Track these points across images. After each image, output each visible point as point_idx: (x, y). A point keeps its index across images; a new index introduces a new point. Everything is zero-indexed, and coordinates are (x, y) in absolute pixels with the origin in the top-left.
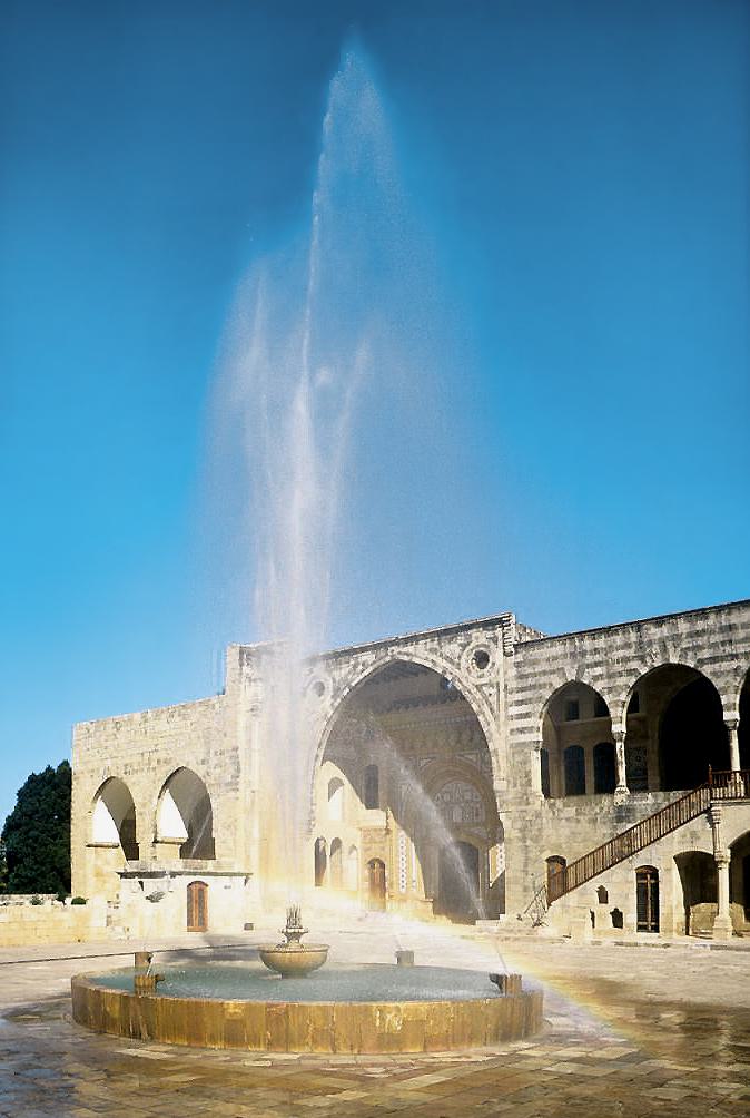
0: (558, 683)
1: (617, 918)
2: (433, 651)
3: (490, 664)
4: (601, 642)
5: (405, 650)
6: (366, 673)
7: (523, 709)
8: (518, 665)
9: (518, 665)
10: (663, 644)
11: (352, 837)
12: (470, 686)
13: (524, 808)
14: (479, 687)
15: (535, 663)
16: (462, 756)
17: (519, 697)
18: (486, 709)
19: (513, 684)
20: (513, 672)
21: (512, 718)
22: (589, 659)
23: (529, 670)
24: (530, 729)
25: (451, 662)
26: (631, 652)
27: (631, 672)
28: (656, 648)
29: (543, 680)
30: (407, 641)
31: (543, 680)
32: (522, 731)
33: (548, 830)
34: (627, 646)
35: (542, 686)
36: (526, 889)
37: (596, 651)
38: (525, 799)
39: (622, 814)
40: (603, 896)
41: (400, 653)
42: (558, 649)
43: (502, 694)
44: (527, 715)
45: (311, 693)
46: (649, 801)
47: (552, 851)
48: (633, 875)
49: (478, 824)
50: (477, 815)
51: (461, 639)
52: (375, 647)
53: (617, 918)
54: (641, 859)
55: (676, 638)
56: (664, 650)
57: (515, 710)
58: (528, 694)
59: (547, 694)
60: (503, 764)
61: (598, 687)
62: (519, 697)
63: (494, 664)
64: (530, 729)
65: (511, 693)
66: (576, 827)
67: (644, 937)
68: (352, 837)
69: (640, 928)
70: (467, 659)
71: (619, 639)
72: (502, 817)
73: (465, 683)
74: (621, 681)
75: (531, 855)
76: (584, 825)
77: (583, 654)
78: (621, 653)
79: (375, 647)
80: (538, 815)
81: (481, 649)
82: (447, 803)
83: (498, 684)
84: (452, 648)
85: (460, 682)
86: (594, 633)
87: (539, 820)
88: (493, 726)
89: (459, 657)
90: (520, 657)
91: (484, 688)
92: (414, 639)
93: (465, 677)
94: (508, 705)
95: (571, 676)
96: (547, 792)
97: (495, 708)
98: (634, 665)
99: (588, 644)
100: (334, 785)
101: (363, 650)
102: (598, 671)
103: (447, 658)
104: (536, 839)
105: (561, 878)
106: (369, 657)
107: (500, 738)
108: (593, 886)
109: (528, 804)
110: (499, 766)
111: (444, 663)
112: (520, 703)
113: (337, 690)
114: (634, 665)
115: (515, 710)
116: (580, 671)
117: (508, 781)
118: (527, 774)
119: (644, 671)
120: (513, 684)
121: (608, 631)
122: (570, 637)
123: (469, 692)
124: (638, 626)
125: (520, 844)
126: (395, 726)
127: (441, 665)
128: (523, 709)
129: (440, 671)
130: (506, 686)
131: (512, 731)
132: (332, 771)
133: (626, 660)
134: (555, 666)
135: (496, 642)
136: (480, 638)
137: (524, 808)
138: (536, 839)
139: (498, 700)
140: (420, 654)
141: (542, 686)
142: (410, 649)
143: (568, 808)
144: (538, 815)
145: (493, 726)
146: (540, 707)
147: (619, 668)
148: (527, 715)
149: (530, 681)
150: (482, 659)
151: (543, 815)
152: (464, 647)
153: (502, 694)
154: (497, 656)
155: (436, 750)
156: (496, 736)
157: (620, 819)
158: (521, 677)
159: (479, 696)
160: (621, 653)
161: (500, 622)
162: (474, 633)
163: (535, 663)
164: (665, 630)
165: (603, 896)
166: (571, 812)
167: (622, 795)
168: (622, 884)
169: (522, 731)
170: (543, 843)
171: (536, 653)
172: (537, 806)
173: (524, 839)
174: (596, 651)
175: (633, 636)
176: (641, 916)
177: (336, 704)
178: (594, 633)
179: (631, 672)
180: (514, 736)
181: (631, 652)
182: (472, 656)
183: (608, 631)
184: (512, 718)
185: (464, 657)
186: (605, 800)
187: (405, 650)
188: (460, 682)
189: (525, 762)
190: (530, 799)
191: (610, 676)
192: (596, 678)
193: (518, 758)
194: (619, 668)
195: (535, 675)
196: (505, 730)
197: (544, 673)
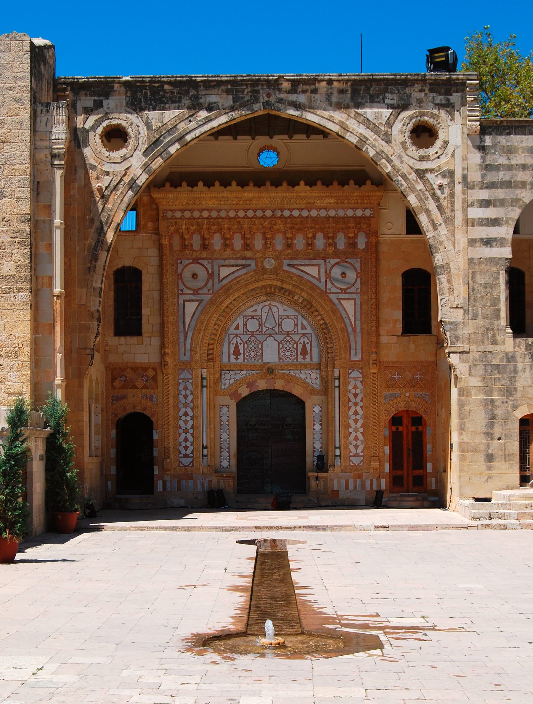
3: (439, 143)
5: (293, 97)
6: (215, 124)
7: (490, 213)
12: (405, 169)
13: (491, 348)
14: (421, 174)
16: (293, 266)
17: (484, 194)
18: (432, 205)
21: (469, 223)
23: (502, 160)
24: (501, 242)
25: (375, 129)
32: (488, 242)
33: (524, 380)
41: (280, 101)
43: (458, 188)
44: (495, 222)
47: (529, 406)
49: (305, 366)
50: (304, 352)
57: (476, 213)
58: (500, 193)
62: (484, 194)
63: (446, 143)
64: (501, 242)
65: (473, 188)
72: (454, 359)
73: (396, 162)
75: (500, 412)
81: (426, 118)
82: (253, 334)
83: (450, 174)
85: (390, 161)
87: (511, 366)
88: (443, 230)
89: (389, 124)
91: (429, 176)
94: (467, 205)
97: (445, 203)
103: (367, 123)
104: (509, 391)
109: (494, 343)
110: (450, 288)
111: (362, 130)
112: (486, 203)
115: (476, 213)
117: (466, 311)
118: (495, 301)
120: (475, 176)
123: (404, 177)
125: (482, 396)
126: (183, 211)
128: (490, 213)
129: (354, 140)
130: (465, 177)
131: (472, 242)
137: (491, 348)
139: (452, 195)
142: (302, 98)
144: (511, 358)
145: (443, 230)
148: (495, 222)
149: (502, 176)
150: (423, 134)
151: (519, 360)
153: (458, 188)
155: (249, 254)
156: (447, 243)
158: (487, 167)
159: (420, 186)
163: (510, 151)
169: (488, 242)
170: (518, 395)
173: (488, 391)
177: (155, 166)
182: (410, 126)
184: (469, 223)
185: (398, 126)
187: (293, 97)
188: (390, 161)
190: (499, 338)
193: (481, 279)
195: (510, 168)
196: (462, 240)
197: (524, 167)
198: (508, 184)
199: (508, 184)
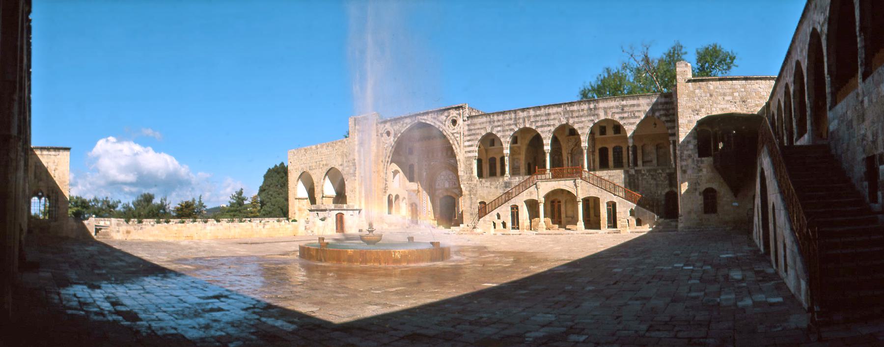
0: (484, 133)
1: (504, 224)
2: (435, 118)
4: (501, 117)
7: (470, 143)
8: (468, 125)
9: (468, 125)
10: (524, 119)
11: (403, 194)
15: (474, 124)
17: (468, 138)
19: (466, 133)
20: (466, 128)
22: (496, 124)
23: (472, 127)
24: (473, 151)
26: (512, 122)
27: (511, 130)
28: (521, 121)
29: (478, 131)
30: (424, 114)
31: (478, 131)
32: (469, 152)
34: (510, 119)
35: (478, 134)
36: (472, 214)
37: (499, 121)
38: (470, 179)
39: (507, 185)
40: (499, 216)
42: (484, 119)
44: (471, 146)
45: (385, 135)
46: (517, 180)
48: (510, 209)
51: (446, 114)
52: (410, 117)
53: (504, 224)
54: (512, 202)
55: (529, 117)
56: (524, 121)
57: (467, 144)
58: (472, 137)
59: (479, 137)
60: (462, 165)
61: (499, 135)
62: (468, 138)
64: (473, 151)
66: (489, 190)
67: (516, 232)
68: (403, 194)
69: (513, 228)
70: (449, 123)
71: (507, 116)
72: (462, 186)
74: (507, 133)
76: (493, 190)
77: (494, 122)
78: (508, 122)
79: (410, 117)
80: (476, 185)
84: (443, 117)
86: (498, 113)
90: (469, 122)
92: (427, 113)
93: (448, 130)
95: (489, 131)
96: (480, 175)
98: (513, 127)
99: (496, 118)
100: (395, 173)
101: (406, 117)
102: (499, 128)
104: (475, 195)
105: (483, 210)
106: (408, 120)
107: (461, 156)
108: (495, 212)
111: (438, 123)
112: (469, 141)
113: (395, 134)
114: (513, 127)
115: (467, 144)
116: (492, 128)
118: (472, 169)
119: (516, 129)
121: (504, 113)
122: (489, 115)
124: (515, 111)
127: (438, 124)
128: (470, 143)
132: (394, 167)
133: (510, 125)
134: (483, 126)
135: (459, 114)
136: (454, 113)
138: (475, 195)
140: (429, 120)
141: (478, 134)
142: (425, 117)
143: (486, 183)
144: (476, 185)
146: (476, 142)
147: (507, 128)
148: (471, 146)
149: (473, 132)
150: (454, 122)
152: (447, 117)
154: (460, 121)
157: (506, 187)
158: (469, 130)
160: (508, 122)
161: (461, 107)
162: (451, 111)
163: (474, 124)
164: (525, 114)
165: (499, 216)
166: (488, 184)
167: (507, 176)
168: (505, 211)
169: (469, 152)
171: (476, 120)
172: (475, 182)
174: (499, 121)
175: (513, 115)
176: (513, 223)
178: (498, 113)
179: (511, 130)
180: (466, 154)
181: (512, 122)
183: (504, 113)
186: (501, 180)
189: (471, 164)
191: (504, 131)
192: (498, 132)
194: (507, 128)
198: (474, 134)
199: (474, 134)
